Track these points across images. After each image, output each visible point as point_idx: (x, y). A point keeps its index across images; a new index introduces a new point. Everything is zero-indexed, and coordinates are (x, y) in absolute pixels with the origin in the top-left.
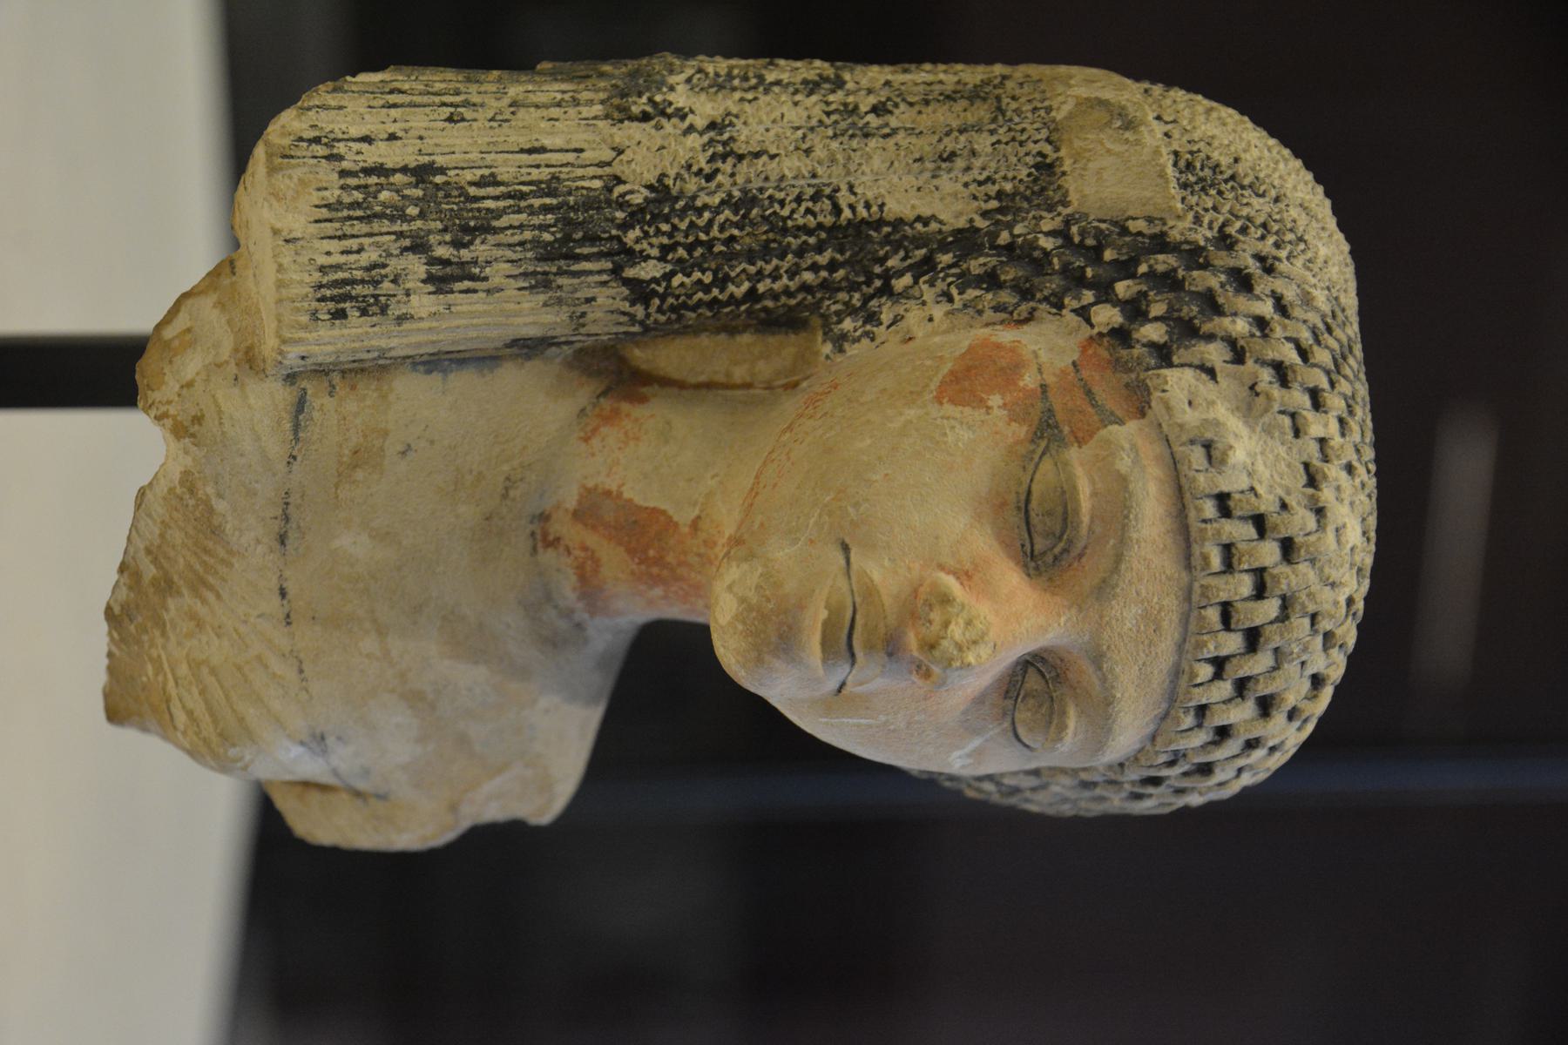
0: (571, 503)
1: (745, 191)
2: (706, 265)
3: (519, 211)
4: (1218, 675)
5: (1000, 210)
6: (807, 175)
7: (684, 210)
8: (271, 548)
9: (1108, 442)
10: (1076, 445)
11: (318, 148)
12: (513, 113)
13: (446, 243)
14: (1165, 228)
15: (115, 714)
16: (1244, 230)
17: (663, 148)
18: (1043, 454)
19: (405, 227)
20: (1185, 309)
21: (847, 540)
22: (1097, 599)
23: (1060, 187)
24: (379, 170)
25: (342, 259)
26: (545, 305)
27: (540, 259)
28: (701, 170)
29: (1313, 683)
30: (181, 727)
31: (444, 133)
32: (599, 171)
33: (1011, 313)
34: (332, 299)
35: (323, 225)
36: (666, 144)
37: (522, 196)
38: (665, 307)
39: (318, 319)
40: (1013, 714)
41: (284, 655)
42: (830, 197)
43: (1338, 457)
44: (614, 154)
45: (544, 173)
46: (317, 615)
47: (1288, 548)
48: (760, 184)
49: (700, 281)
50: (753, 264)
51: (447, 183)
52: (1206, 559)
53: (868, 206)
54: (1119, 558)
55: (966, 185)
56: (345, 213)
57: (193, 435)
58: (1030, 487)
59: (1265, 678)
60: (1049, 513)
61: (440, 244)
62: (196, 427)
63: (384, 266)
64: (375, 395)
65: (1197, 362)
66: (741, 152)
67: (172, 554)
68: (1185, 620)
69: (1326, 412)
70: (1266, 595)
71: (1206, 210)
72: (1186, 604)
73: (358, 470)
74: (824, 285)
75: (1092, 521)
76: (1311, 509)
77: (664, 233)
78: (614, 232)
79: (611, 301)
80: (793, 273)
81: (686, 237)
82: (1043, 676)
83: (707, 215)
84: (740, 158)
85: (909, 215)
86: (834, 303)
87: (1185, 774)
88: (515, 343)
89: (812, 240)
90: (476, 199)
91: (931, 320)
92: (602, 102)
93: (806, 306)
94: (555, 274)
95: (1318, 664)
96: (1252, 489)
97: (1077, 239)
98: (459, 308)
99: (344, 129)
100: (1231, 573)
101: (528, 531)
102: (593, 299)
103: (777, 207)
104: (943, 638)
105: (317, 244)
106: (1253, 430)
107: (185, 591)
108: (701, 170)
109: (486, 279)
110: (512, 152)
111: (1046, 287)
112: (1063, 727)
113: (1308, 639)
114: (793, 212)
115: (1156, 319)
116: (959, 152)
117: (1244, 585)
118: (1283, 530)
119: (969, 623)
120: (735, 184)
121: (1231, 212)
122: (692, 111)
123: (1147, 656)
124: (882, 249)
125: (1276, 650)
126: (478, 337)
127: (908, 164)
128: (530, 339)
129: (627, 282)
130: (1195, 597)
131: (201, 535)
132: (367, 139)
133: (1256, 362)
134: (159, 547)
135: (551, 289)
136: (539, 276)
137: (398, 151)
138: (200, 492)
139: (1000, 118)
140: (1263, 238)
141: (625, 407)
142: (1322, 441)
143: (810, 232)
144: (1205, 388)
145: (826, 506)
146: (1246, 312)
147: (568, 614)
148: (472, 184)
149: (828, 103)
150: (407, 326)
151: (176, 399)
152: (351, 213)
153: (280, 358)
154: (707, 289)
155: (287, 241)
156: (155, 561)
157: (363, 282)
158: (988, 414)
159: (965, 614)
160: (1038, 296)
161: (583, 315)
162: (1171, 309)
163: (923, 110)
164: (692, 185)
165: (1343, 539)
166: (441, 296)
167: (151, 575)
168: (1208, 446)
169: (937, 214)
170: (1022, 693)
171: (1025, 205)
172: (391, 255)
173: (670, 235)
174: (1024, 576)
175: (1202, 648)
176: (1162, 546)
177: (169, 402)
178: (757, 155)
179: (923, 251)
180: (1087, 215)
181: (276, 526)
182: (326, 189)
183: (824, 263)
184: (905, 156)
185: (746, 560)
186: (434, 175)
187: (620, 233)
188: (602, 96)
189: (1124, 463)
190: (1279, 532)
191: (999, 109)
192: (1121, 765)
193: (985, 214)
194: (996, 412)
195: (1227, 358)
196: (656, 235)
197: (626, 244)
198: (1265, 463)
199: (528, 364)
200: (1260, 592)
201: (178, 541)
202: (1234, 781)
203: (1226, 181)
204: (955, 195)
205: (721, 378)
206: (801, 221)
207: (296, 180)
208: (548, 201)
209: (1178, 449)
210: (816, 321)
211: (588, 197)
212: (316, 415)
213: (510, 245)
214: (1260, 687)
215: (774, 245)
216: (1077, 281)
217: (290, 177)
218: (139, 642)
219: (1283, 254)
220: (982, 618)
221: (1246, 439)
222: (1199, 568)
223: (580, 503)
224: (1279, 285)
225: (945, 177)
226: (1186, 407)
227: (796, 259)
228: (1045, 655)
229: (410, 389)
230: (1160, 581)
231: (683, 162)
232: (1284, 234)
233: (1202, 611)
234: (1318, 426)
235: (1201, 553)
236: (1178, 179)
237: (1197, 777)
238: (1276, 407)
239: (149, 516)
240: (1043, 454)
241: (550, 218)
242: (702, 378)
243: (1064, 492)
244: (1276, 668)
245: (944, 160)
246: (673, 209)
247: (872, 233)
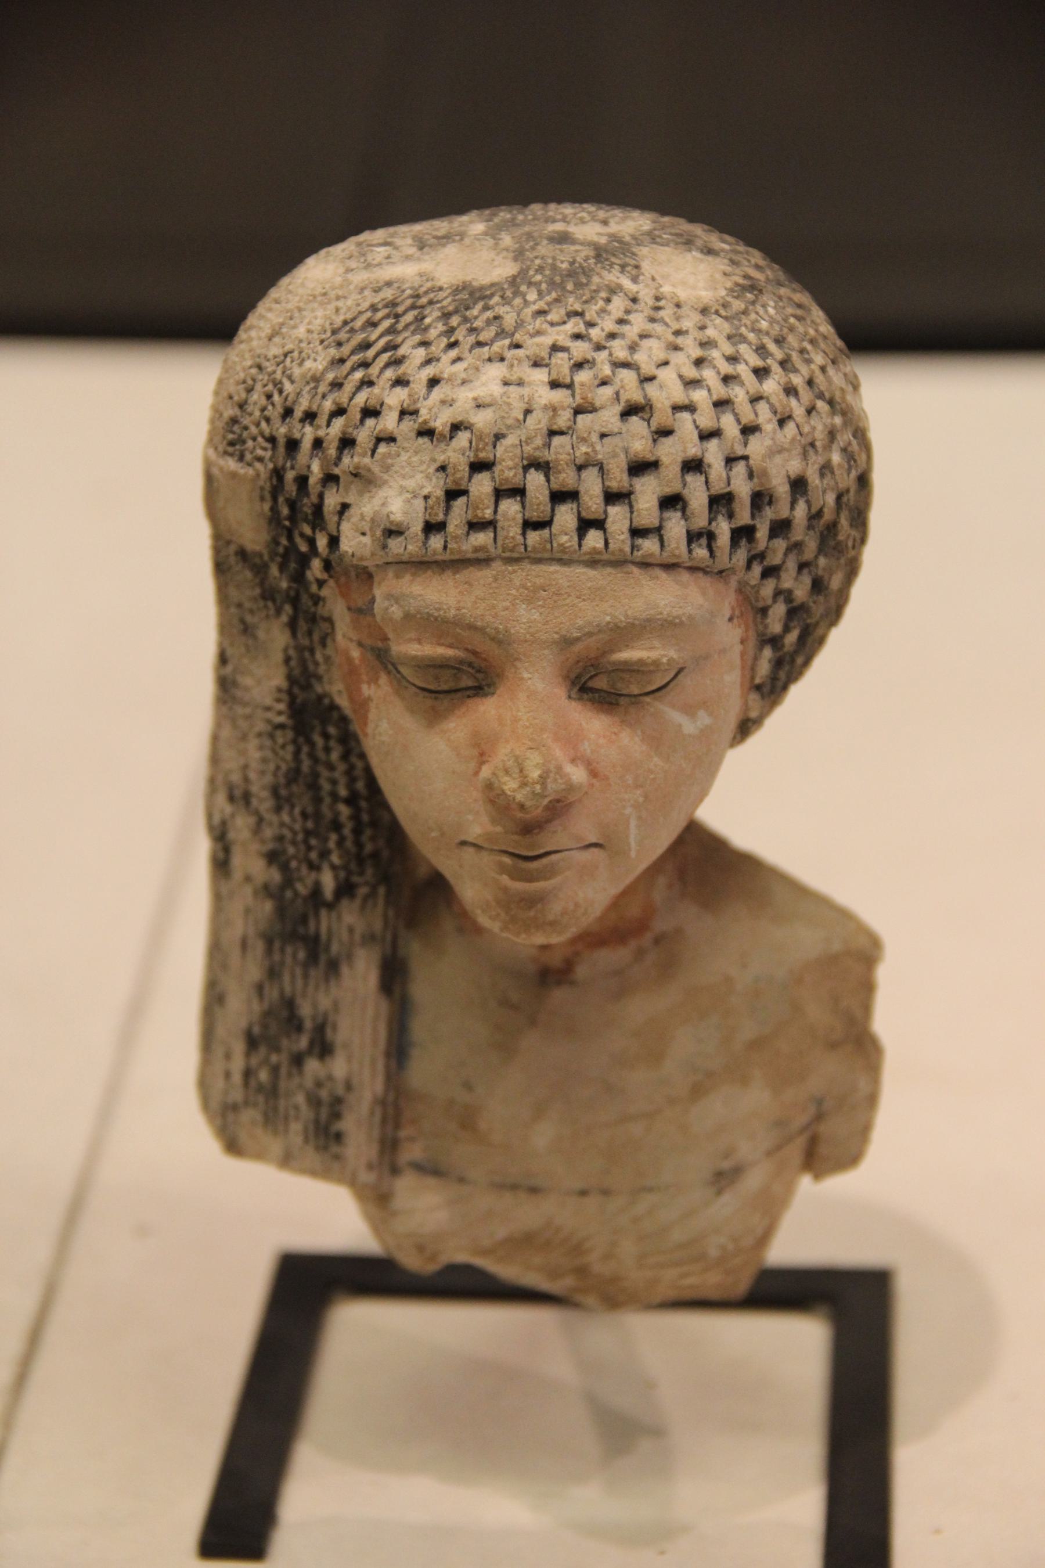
4: (599, 524)
16: (268, 420)
18: (396, 669)
21: (457, 841)
22: (509, 644)
33: (327, 635)
40: (635, 696)
43: (415, 402)
47: (479, 466)
52: (476, 550)
53: (278, 700)
54: (472, 627)
60: (437, 678)
65: (336, 518)
68: (539, 561)
69: (382, 404)
70: (522, 486)
75: (442, 645)
76: (451, 438)
80: (331, 767)
89: (305, 749)
96: (426, 498)
104: (514, 799)
112: (641, 662)
113: (574, 437)
115: (314, 532)
117: (510, 507)
118: (458, 476)
119: (507, 771)
123: (569, 596)
130: (515, 555)
140: (273, 405)
142: (403, 413)
144: (353, 513)
146: (307, 457)
159: (501, 774)
162: (306, 520)
164: (268, 833)
165: (488, 400)
170: (613, 691)
175: (565, 548)
176: (466, 586)
189: (396, 612)
190: (461, 478)
195: (335, 490)
200: (519, 492)
206: (289, 757)
216: (299, 577)
222: (488, 554)
224: (298, 413)
228: (573, 676)
230: (497, 588)
233: (529, 549)
234: (389, 421)
237: (736, 506)
238: (367, 460)
241: (289, 950)
243: (419, 667)
244: (601, 467)
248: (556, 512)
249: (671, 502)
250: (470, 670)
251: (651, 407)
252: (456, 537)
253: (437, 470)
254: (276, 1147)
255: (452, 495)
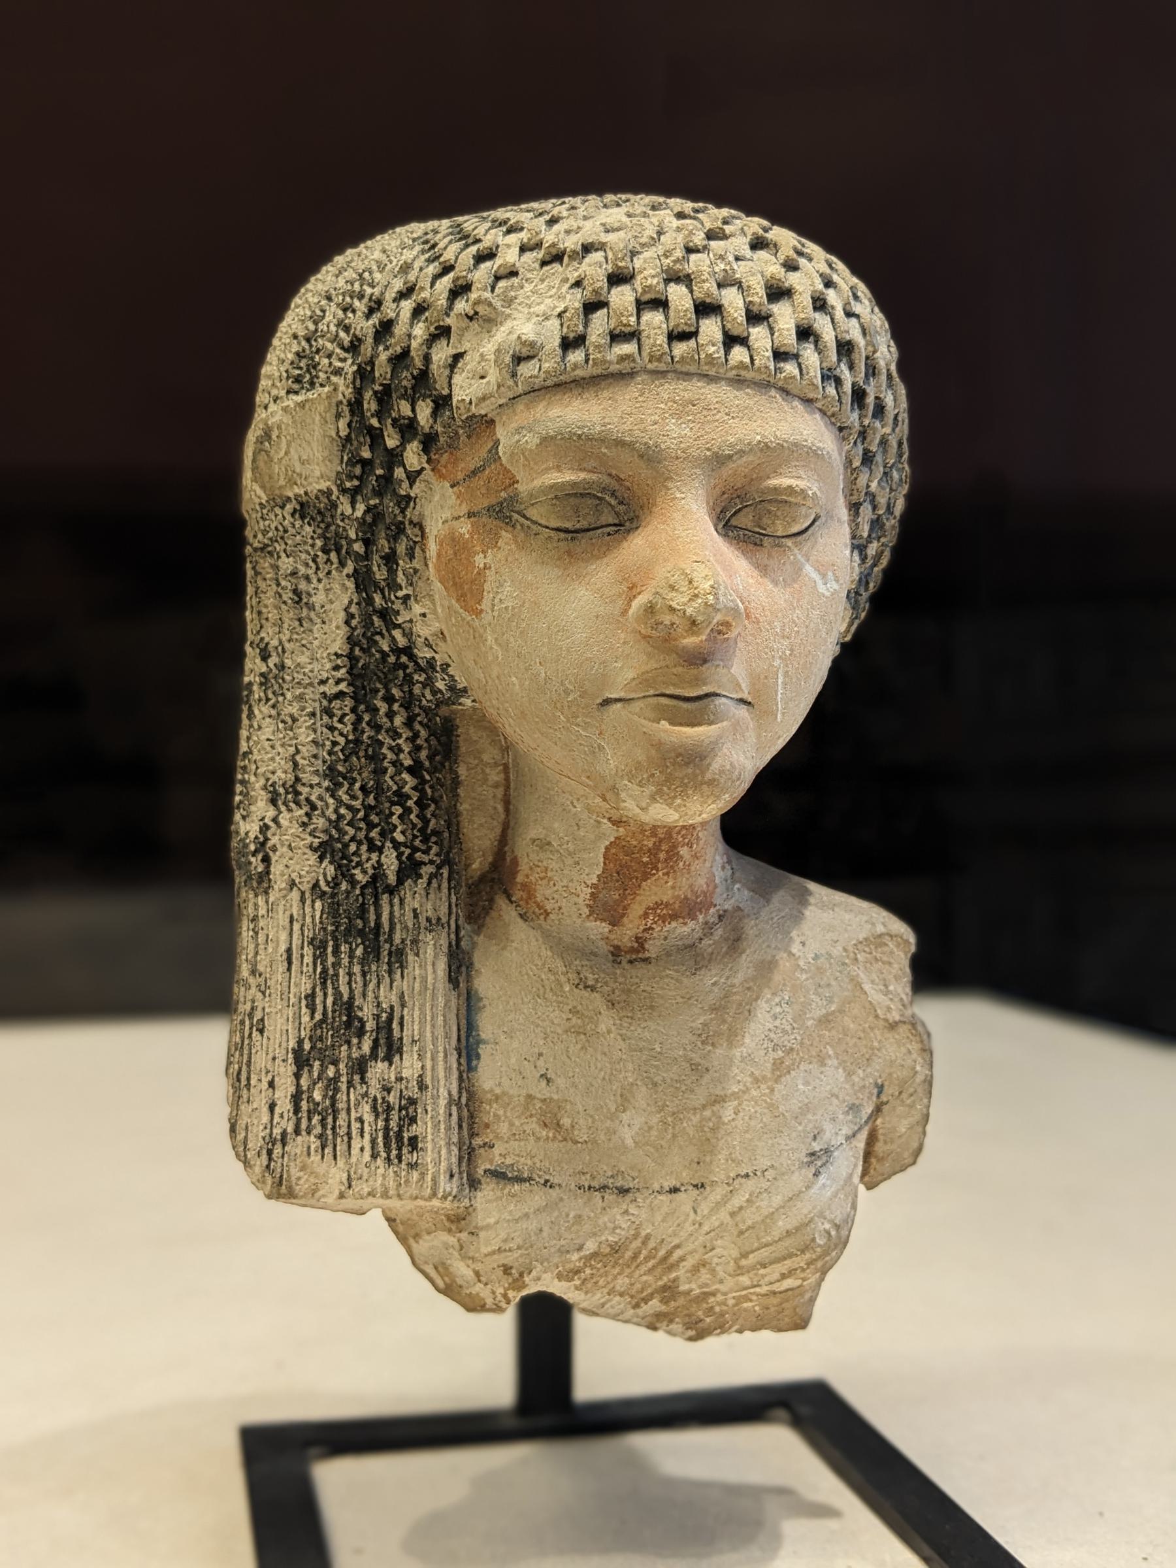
0: (605, 928)
1: (325, 776)
2: (387, 812)
3: (337, 975)
4: (743, 341)
5: (338, 551)
6: (312, 721)
7: (339, 830)
8: (631, 1201)
9: (512, 455)
10: (516, 486)
11: (275, 1151)
12: (260, 975)
13: (360, 1042)
14: (345, 402)
15: (801, 1323)
16: (347, 329)
17: (290, 845)
18: (524, 516)
19: (344, 1079)
20: (405, 383)
21: (599, 701)
23: (317, 498)
24: (296, 1099)
25: (367, 1137)
26: (417, 955)
27: (378, 958)
28: (307, 814)
29: (761, 249)
30: (799, 1282)
31: (272, 1038)
32: (308, 902)
33: (415, 543)
34: (400, 1149)
35: (338, 1153)
36: (287, 843)
37: (325, 971)
38: (424, 848)
39: (416, 1163)
40: (778, 537)
41: (731, 1191)
42: (330, 701)
44: (295, 888)
45: (308, 951)
46: (696, 1160)
47: (617, 278)
48: (320, 762)
49: (400, 817)
50: (386, 769)
51: (311, 1038)
52: (622, 359)
53: (336, 668)
54: (620, 443)
55: (319, 581)
56: (329, 1132)
57: (521, 1275)
58: (553, 529)
59: (748, 296)
61: (360, 1048)
62: (514, 1271)
63: (375, 1099)
64: (495, 1105)
65: (447, 372)
66: (293, 778)
67: (638, 1286)
68: (687, 376)
69: (498, 247)
70: (664, 298)
71: (330, 364)
72: (670, 376)
73: (561, 1122)
74: (407, 706)
75: (585, 470)
76: (583, 257)
77: (358, 848)
78: (358, 892)
79: (417, 895)
80: (396, 735)
81: (361, 829)
82: (740, 510)
83: (342, 811)
84: (297, 779)
85: (343, 631)
86: (424, 697)
87: (851, 367)
88: (453, 980)
89: (366, 717)
90: (325, 1013)
91: (424, 615)
92: (256, 896)
93: (430, 720)
94: (392, 945)
95: (740, 244)
96: (560, 315)
97: (356, 483)
98: (416, 1033)
99: (261, 1127)
100: (640, 333)
101: (627, 966)
102: (415, 910)
103: (337, 749)
104: (684, 613)
105: (353, 1160)
106: (509, 316)
107: (673, 1275)
108: (307, 814)
109: (392, 1007)
110: (290, 978)
111: (393, 512)
112: (790, 490)
113: (711, 255)
114: (341, 734)
115: (413, 410)
116: (294, 587)
117: (653, 319)
118: (599, 284)
119: (672, 588)
120: (319, 784)
121: (332, 342)
122: (262, 819)
123: (719, 412)
124: (374, 655)
125: (720, 286)
126: (444, 1016)
127: (304, 632)
128: (450, 967)
129: (400, 882)
130: (662, 367)
131: (621, 1261)
132: (272, 1107)
133: (448, 315)
134: (632, 1297)
135: (404, 948)
136: (393, 959)
137: (283, 1081)
138: (577, 1264)
139: (270, 549)
141: (520, 878)
142: (523, 249)
143: (359, 719)
144: (470, 363)
145: (568, 721)
146: (407, 326)
147: (708, 928)
148: (312, 1018)
149: (260, 700)
150: (428, 1080)
151: (489, 1286)
152: (329, 1127)
153: (450, 1198)
154: (407, 811)
155: (350, 1187)
156: (646, 1300)
157: (387, 1120)
158: (490, 568)
160: (400, 518)
161: (428, 920)
162: (404, 396)
163: (265, 616)
164: (320, 823)
165: (616, 225)
166: (405, 1049)
167: (659, 1304)
168: (518, 359)
169: (344, 607)
170: (757, 530)
171: (333, 528)
172: (367, 1092)
173: (360, 843)
174: (637, 533)
177: (493, 1293)
178: (296, 764)
179: (375, 618)
180: (338, 473)
181: (610, 1197)
182: (309, 1148)
183: (387, 706)
184: (297, 634)
185: (618, 794)
186: (303, 1050)
187: (358, 887)
188: (251, 896)
189: (530, 440)
190: (601, 288)
191: (262, 549)
192: (841, 429)
193: (342, 564)
194: (488, 560)
196: (360, 856)
197: (367, 882)
198: (538, 304)
199: (477, 965)
200: (660, 304)
201: (627, 1280)
202: (862, 320)
203: (311, 346)
204: (327, 590)
205: (500, 792)
206: (350, 727)
207: (302, 1174)
208: (330, 949)
209: (520, 389)
210: (444, 711)
211: (329, 913)
212: (508, 1161)
213: (365, 985)
214: (756, 299)
215: (370, 752)
217: (299, 1179)
218: (722, 1314)
219: (369, 290)
220: (669, 575)
221: (515, 323)
222: (632, 365)
223: (603, 920)
224: (390, 295)
225: (314, 599)
226: (484, 381)
227: (383, 731)
228: (719, 510)
229: (487, 1077)
231: (301, 829)
232: (354, 291)
233: (676, 359)
234: (509, 256)
235: (618, 363)
236: (308, 390)
237: (855, 356)
239: (603, 1305)
240: (524, 516)
241: (344, 948)
242: (500, 808)
244: (739, 284)
245: (301, 599)
246: (338, 840)
247: (360, 665)
248: (701, 324)
249: (805, 333)
250: (613, 502)
251: (775, 245)
252: (598, 347)
253: (571, 287)
254: (336, 1175)
255: (591, 307)
